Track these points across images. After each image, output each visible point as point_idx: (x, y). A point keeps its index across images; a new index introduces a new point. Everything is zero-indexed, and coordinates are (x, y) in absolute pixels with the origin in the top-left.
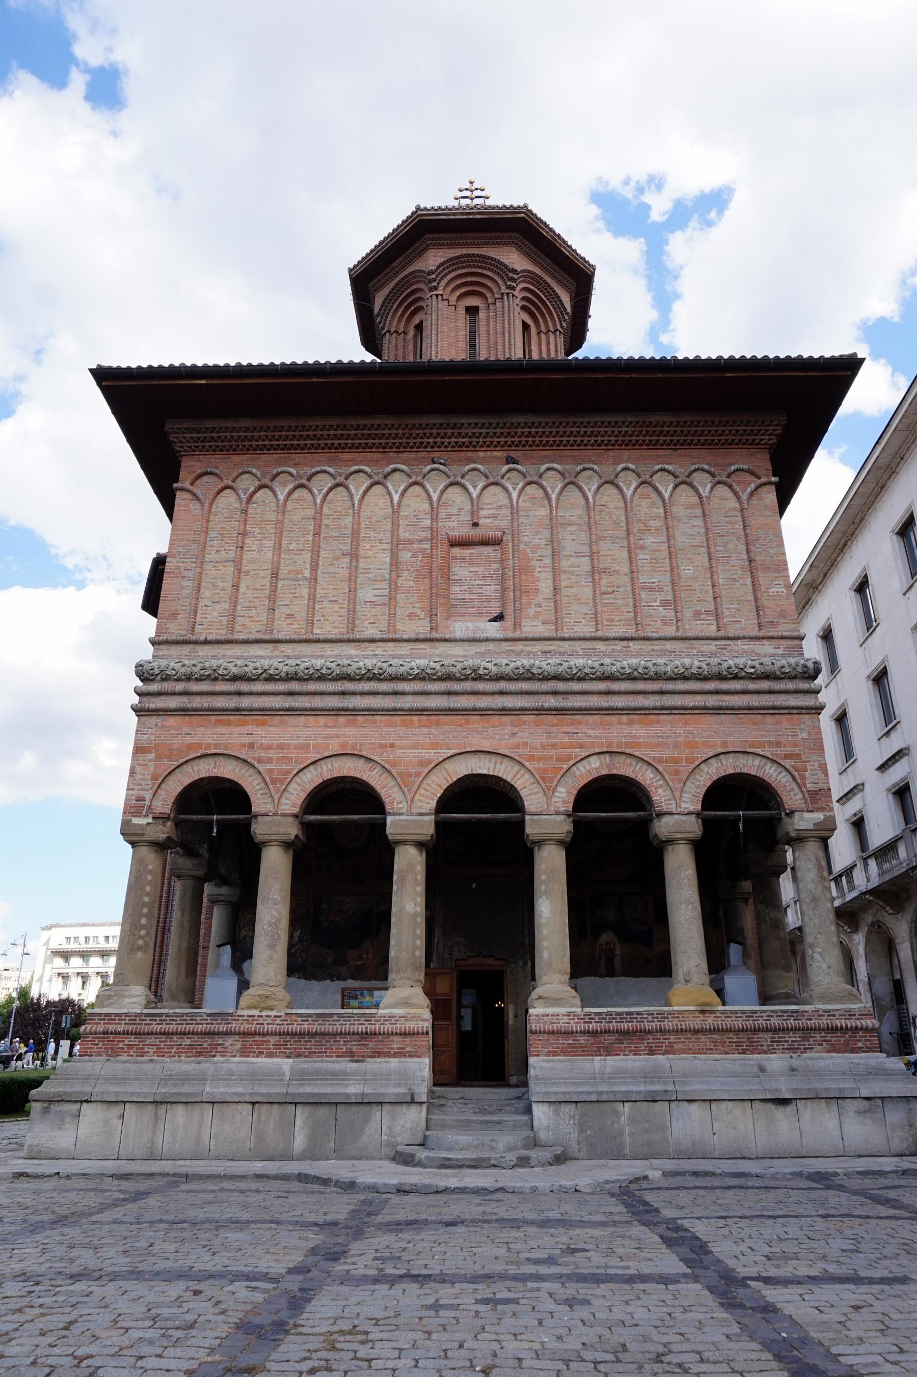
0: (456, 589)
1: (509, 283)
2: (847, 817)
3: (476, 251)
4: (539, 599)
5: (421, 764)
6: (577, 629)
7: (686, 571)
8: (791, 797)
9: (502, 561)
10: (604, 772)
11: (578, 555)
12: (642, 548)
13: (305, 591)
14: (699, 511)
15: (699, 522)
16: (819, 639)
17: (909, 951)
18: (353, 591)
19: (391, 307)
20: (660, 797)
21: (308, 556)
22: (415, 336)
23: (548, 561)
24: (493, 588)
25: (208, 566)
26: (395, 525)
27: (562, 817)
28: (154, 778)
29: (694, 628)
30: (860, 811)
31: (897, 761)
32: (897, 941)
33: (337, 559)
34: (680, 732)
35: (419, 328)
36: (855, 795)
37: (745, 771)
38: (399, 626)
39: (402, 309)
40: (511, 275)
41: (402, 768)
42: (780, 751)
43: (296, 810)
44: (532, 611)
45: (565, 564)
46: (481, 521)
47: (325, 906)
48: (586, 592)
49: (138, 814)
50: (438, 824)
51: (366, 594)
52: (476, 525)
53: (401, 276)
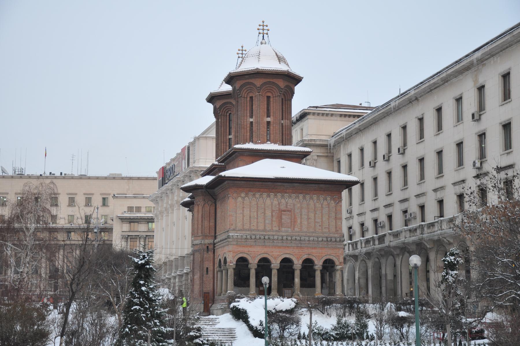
0: (283, 221)
1: (280, 92)
2: (359, 221)
3: (271, 80)
4: (297, 224)
5: (277, 255)
6: (304, 230)
7: (324, 219)
8: (337, 263)
9: (291, 215)
10: (307, 258)
11: (305, 215)
12: (316, 214)
13: (256, 220)
14: (327, 206)
15: (327, 209)
16: (359, 150)
17: (371, 272)
18: (265, 221)
19: (243, 88)
20: (316, 262)
21: (256, 213)
22: (250, 100)
23: (299, 216)
24: (289, 221)
25: (237, 214)
26: (272, 207)
27: (300, 265)
28: (233, 257)
29: (324, 230)
30: (363, 221)
31: (375, 211)
32: (368, 268)
33: (261, 214)
34: (320, 251)
35: (251, 98)
36: (363, 215)
37: (330, 258)
38: (273, 229)
39: (246, 90)
40: (281, 90)
41: (274, 256)
42: (336, 255)
43: (257, 263)
44: (296, 226)
45: (303, 216)
46: (288, 207)
47: (241, 272)
48: (306, 223)
49: (231, 263)
50: (280, 265)
51: (267, 222)
52: (287, 207)
53: (247, 81)
